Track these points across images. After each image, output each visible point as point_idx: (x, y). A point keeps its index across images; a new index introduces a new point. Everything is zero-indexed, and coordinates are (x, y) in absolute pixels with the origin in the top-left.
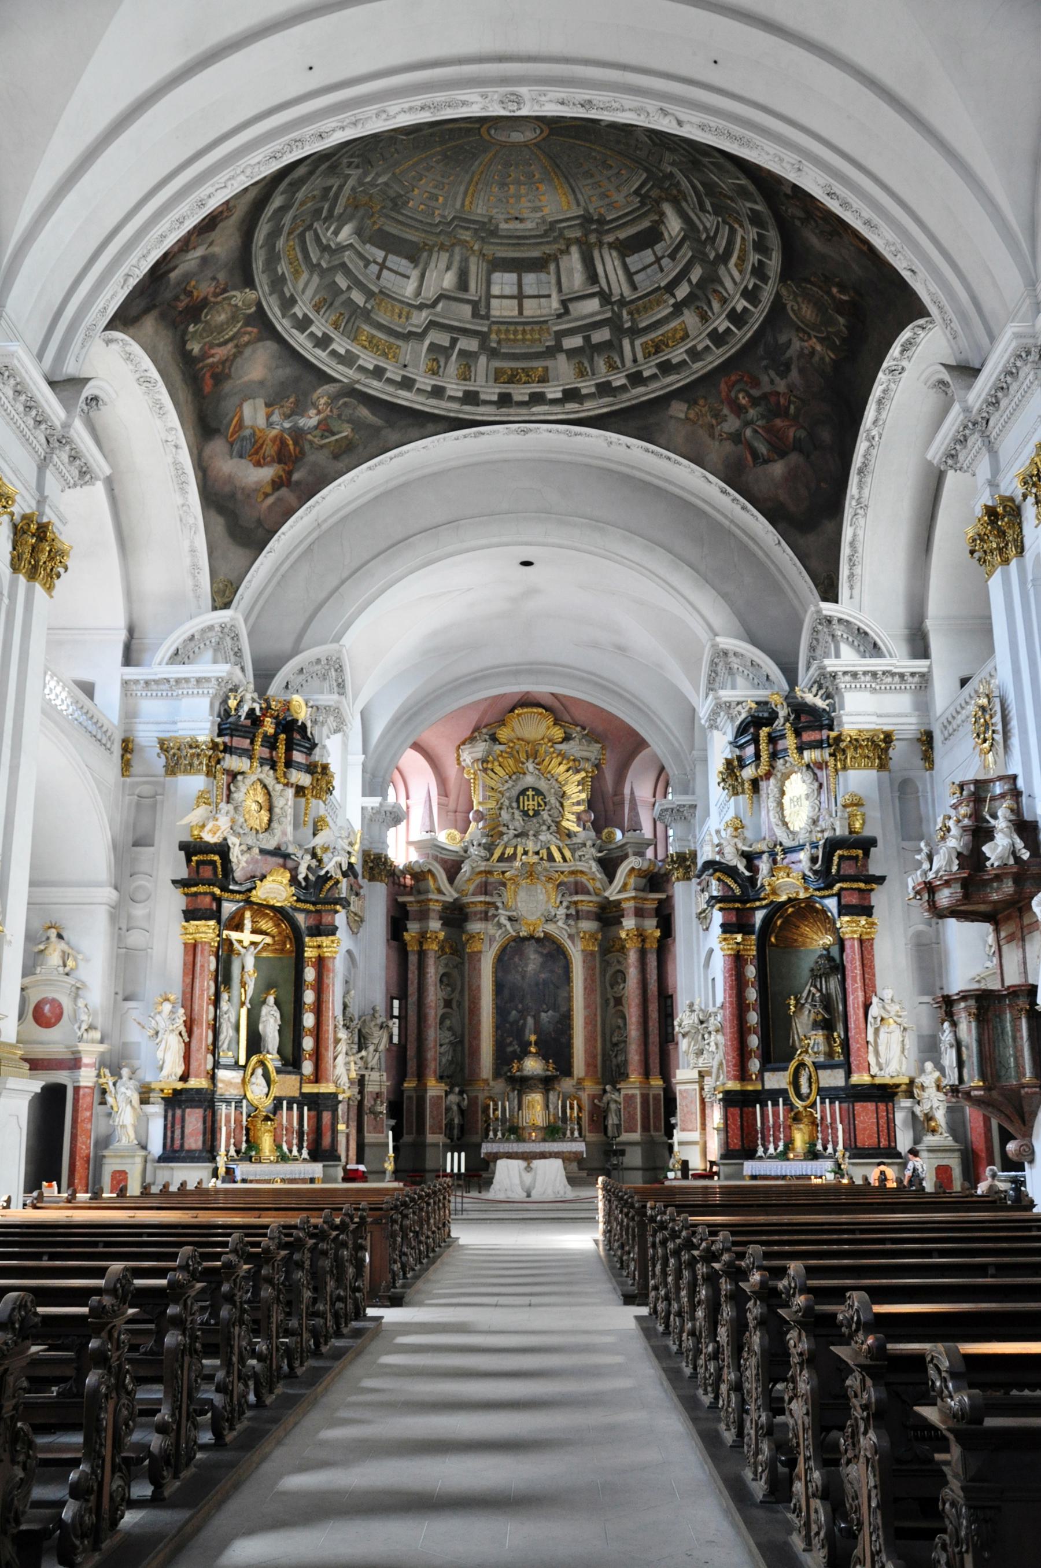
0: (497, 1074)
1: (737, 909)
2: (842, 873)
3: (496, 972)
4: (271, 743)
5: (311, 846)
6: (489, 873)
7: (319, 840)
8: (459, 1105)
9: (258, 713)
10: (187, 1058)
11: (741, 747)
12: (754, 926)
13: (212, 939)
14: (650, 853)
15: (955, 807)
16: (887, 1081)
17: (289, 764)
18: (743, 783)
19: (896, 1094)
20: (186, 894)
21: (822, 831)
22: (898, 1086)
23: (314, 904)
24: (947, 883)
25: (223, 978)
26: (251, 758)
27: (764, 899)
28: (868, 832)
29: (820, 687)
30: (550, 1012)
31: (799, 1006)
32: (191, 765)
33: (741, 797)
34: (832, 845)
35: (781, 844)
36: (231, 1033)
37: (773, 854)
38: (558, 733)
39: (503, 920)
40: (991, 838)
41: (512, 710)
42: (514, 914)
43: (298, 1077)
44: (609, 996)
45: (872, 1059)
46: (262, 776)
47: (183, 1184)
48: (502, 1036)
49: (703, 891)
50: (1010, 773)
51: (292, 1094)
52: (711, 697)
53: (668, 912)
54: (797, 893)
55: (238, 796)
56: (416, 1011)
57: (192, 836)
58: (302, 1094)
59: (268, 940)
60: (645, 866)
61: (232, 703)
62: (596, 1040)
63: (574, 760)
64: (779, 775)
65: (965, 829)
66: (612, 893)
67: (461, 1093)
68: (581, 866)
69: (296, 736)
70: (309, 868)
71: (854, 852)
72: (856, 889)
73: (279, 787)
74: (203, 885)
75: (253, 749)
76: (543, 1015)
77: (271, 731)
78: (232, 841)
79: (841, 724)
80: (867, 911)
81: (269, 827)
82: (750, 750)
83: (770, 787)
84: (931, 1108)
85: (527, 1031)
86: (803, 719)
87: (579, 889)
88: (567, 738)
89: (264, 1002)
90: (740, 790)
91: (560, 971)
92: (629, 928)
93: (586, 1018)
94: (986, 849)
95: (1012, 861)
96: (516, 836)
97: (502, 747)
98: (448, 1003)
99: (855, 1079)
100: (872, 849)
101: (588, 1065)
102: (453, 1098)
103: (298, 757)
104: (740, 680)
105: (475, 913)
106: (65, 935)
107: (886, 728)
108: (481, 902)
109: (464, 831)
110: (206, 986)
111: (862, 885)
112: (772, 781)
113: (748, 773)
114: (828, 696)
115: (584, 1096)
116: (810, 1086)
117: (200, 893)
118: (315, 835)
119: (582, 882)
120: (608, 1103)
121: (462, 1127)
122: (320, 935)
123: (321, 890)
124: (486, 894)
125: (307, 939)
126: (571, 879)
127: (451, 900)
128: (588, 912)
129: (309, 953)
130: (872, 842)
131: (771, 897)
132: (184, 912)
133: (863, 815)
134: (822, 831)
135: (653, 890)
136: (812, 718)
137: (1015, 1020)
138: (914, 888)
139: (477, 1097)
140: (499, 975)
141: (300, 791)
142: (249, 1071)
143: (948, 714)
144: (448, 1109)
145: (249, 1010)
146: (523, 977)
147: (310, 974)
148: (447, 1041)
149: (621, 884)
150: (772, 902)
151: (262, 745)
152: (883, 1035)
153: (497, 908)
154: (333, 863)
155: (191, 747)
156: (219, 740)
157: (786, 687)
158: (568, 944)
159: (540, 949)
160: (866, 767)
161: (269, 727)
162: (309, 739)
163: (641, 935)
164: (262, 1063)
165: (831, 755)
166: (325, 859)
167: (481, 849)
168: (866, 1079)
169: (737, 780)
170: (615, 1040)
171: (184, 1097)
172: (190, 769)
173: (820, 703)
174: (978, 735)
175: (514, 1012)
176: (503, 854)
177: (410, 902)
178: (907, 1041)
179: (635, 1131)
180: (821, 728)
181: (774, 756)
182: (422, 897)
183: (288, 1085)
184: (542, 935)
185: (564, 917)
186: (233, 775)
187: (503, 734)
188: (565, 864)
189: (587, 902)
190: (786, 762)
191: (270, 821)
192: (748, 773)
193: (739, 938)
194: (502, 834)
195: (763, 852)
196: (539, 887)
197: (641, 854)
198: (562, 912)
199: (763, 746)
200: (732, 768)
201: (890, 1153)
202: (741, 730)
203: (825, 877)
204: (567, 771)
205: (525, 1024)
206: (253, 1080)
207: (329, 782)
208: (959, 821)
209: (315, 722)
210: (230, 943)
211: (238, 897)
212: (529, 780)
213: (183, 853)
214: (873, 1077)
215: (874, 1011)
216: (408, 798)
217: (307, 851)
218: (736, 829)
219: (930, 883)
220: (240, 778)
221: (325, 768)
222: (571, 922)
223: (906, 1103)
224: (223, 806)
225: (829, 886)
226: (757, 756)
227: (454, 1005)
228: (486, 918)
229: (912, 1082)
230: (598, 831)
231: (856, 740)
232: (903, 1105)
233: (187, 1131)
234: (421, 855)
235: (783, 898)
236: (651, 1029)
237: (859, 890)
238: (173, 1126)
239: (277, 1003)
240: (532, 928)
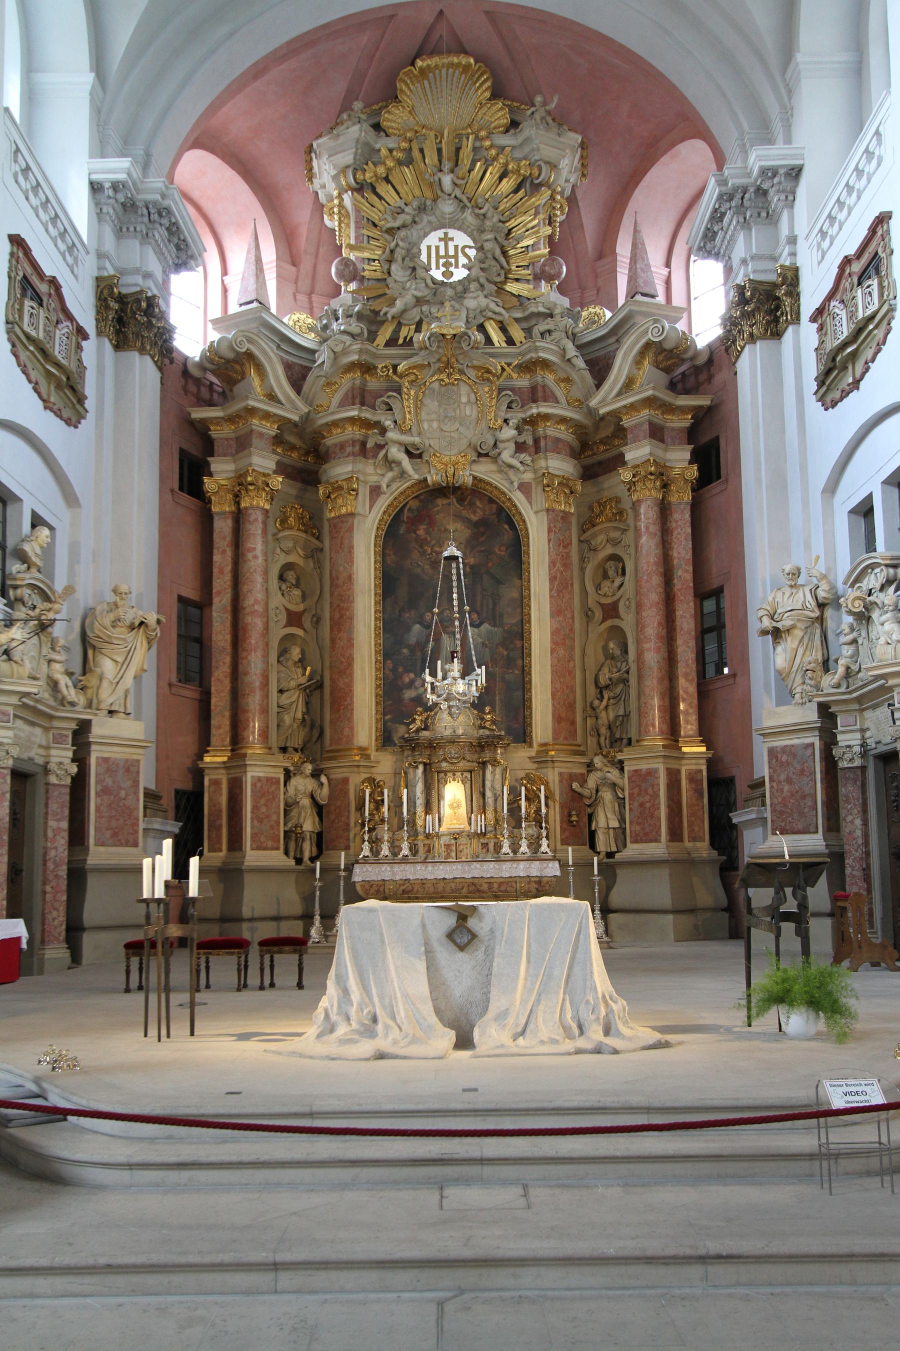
6: (367, 369)
8: (312, 797)
39: (396, 453)
42: (417, 440)
44: (591, 603)
48: (394, 670)
53: (705, 438)
56: (228, 623)
62: (571, 673)
67: (316, 775)
68: (547, 351)
92: (638, 462)
93: (555, 632)
98: (294, 619)
101: (558, 719)
102: (302, 784)
105: (342, 446)
108: (352, 420)
115: (553, 776)
119: (544, 387)
120: (597, 791)
121: (319, 839)
124: (363, 404)
126: (522, 382)
128: (558, 440)
139: (346, 781)
140: (389, 560)
144: (289, 807)
148: (293, 684)
153: (383, 431)
158: (519, 498)
159: (465, 513)
163: (662, 475)
167: (353, 321)
170: (603, 680)
175: (417, 627)
179: (657, 840)
184: (469, 481)
185: (512, 446)
188: (511, 350)
196: (464, 389)
198: (509, 433)
222: (527, 458)
227: (307, 621)
228: (363, 450)
236: (680, 650)
240: (451, 471)
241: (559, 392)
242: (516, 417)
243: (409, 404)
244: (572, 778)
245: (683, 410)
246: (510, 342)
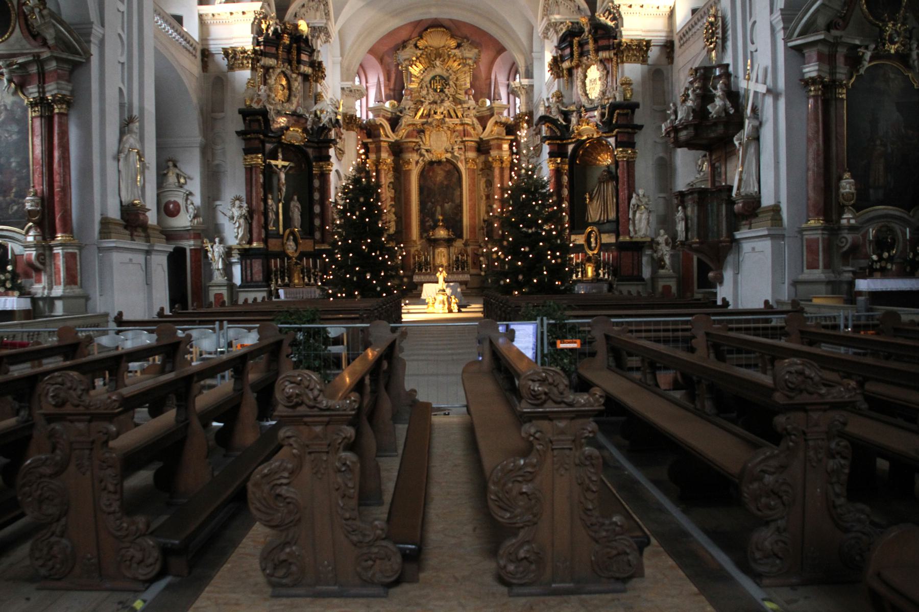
0: (421, 237)
1: (558, 144)
2: (619, 122)
3: (420, 180)
4: (288, 49)
5: (314, 108)
7: (317, 107)
9: (279, 31)
10: (250, 231)
11: (562, 49)
12: (567, 153)
13: (261, 165)
14: (505, 113)
15: (691, 83)
16: (639, 239)
17: (299, 62)
18: (562, 71)
19: (643, 247)
20: (244, 139)
21: (608, 99)
22: (644, 242)
23: (317, 143)
24: (685, 127)
25: (268, 187)
26: (277, 58)
27: (573, 138)
28: (634, 100)
29: (610, 13)
30: (450, 203)
31: (591, 199)
32: (242, 63)
33: (561, 79)
34: (614, 107)
35: (584, 106)
36: (274, 217)
37: (579, 113)
38: (453, 43)
39: (423, 152)
40: (713, 101)
41: (426, 30)
43: (312, 241)
45: (631, 228)
46: (284, 69)
47: (255, 299)
49: (537, 134)
50: (725, 62)
51: (310, 250)
52: (545, 19)
54: (593, 135)
55: (272, 81)
57: (246, 105)
58: (315, 250)
59: (292, 165)
60: (503, 120)
61: (264, 26)
63: (462, 59)
64: (584, 66)
65: (697, 96)
66: (485, 136)
68: (467, 120)
69: (303, 45)
70: (314, 123)
71: (625, 111)
72: (625, 132)
73: (294, 76)
74: (254, 133)
75: (278, 53)
76: (446, 205)
77: (288, 42)
78: (268, 107)
79: (621, 36)
80: (632, 145)
81: (289, 100)
82: (568, 51)
83: (579, 73)
84: (662, 255)
85: (437, 214)
86: (600, 32)
87: (465, 133)
88: (459, 46)
89: (292, 199)
90: (561, 75)
91: (454, 180)
94: (709, 107)
95: (723, 115)
96: (430, 104)
97: (421, 52)
99: (621, 239)
100: (637, 110)
101: (471, 232)
103: (304, 57)
104: (562, 9)
106: (178, 165)
107: (647, 38)
109: (399, 101)
110: (258, 192)
111: (630, 130)
112: (580, 70)
113: (566, 65)
114: (614, 19)
115: (469, 249)
116: (596, 243)
117: (252, 138)
118: (316, 103)
122: (321, 161)
123: (321, 135)
125: (314, 164)
127: (393, 141)
128: (471, 147)
129: (316, 171)
130: (637, 105)
131: (578, 137)
132: (244, 150)
133: (632, 90)
134: (608, 99)
135: (507, 134)
136: (604, 32)
137: (719, 205)
138: (666, 130)
141: (306, 77)
142: (285, 237)
143: (684, 31)
145: (283, 204)
146: (435, 184)
147: (316, 183)
149: (490, 131)
150: (578, 140)
151: (283, 51)
152: (638, 215)
154: (327, 119)
155: (242, 53)
156: (257, 48)
157: (589, 14)
160: (635, 61)
161: (286, 40)
162: (310, 47)
164: (292, 233)
165: (614, 54)
166: (322, 118)
168: (628, 239)
169: (559, 69)
171: (251, 252)
172: (242, 67)
173: (611, 24)
174: (707, 41)
175: (430, 204)
176: (423, 114)
177: (370, 142)
178: (651, 218)
180: (609, 38)
181: (581, 54)
182: (377, 139)
183: (307, 245)
186: (267, 69)
187: (421, 44)
189: (471, 141)
190: (588, 58)
191: (290, 95)
192: (566, 65)
193: (559, 160)
194: (422, 103)
195: (574, 111)
197: (501, 114)
199: (575, 48)
200: (556, 63)
201: (640, 279)
202: (562, 40)
203: (607, 125)
204: (459, 65)
205: (436, 210)
206: (288, 243)
207: (323, 72)
208: (694, 91)
209: (313, 36)
210: (270, 165)
211: (274, 140)
212: (438, 71)
213: (241, 116)
214: (631, 238)
215: (633, 201)
216: (367, 82)
217: (311, 113)
218: (558, 98)
219: (676, 127)
220: (271, 71)
221: (320, 63)
223: (648, 252)
224: (262, 87)
225: (612, 131)
226: (572, 54)
229: (652, 240)
230: (477, 101)
231: (630, 45)
232: (647, 253)
233: (254, 272)
234: (375, 116)
235: (585, 137)
237: (628, 133)
238: (246, 269)
239: (299, 200)
241: (472, 131)
242: (459, 140)
243: (427, 138)
244: (474, 249)
245: (508, 140)
246: (457, 117)
